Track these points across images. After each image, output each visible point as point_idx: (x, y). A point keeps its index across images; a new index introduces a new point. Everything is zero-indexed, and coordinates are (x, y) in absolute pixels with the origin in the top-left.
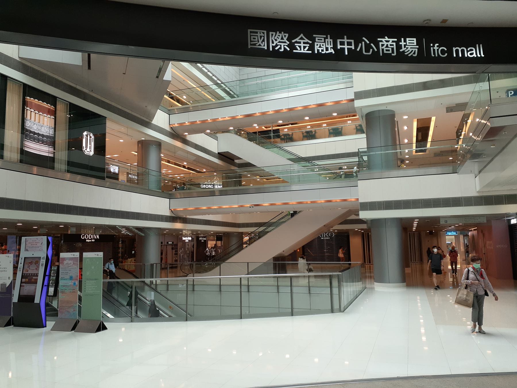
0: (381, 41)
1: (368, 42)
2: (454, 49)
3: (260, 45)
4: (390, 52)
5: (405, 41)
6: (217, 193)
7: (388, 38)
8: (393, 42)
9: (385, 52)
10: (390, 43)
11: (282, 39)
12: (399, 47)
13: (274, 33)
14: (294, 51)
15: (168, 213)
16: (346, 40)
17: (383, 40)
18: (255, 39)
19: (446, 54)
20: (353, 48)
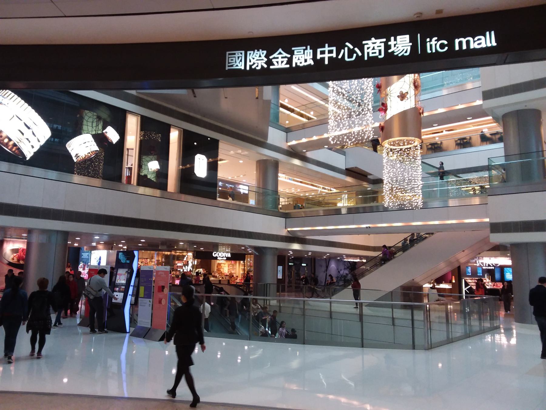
0: (367, 44)
1: (351, 47)
2: (457, 41)
3: (237, 66)
4: (377, 54)
5: (395, 40)
6: (344, 211)
7: (376, 39)
8: (381, 42)
9: (371, 55)
10: (378, 44)
11: (260, 56)
12: (387, 47)
13: (252, 52)
14: (271, 67)
15: (284, 233)
16: (327, 49)
17: (368, 42)
18: (232, 60)
19: (446, 48)
20: (334, 55)
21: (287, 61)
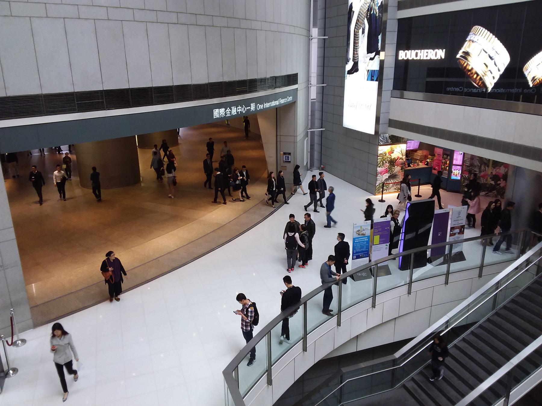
14: (226, 116)
20: (241, 110)
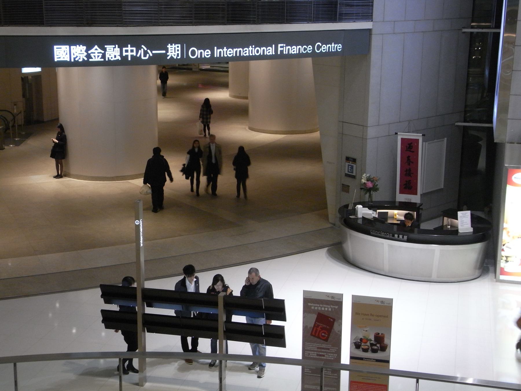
1: (146, 49)
14: (90, 60)
16: (129, 48)
20: (135, 55)
21: (102, 56)
